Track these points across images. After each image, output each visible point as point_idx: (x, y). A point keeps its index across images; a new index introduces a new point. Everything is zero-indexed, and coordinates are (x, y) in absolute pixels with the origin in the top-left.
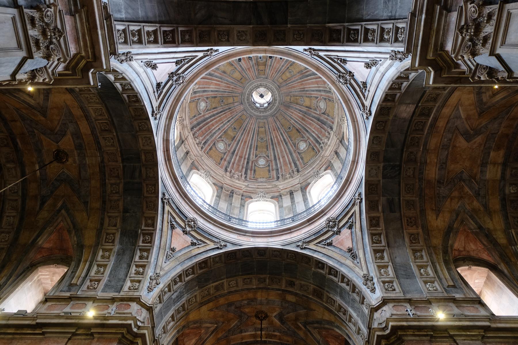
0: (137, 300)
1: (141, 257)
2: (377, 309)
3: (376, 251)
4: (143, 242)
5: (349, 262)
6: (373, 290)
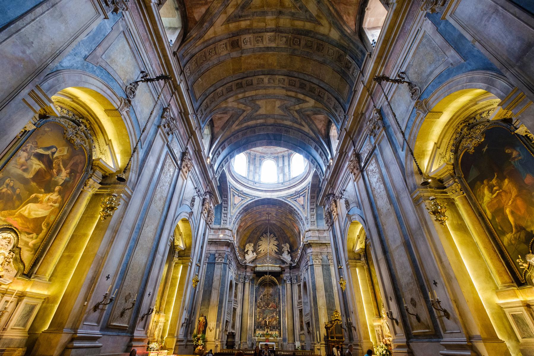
0: (227, 229)
1: (225, 210)
2: (307, 232)
3: (311, 209)
4: (224, 204)
5: (301, 209)
6: (308, 224)
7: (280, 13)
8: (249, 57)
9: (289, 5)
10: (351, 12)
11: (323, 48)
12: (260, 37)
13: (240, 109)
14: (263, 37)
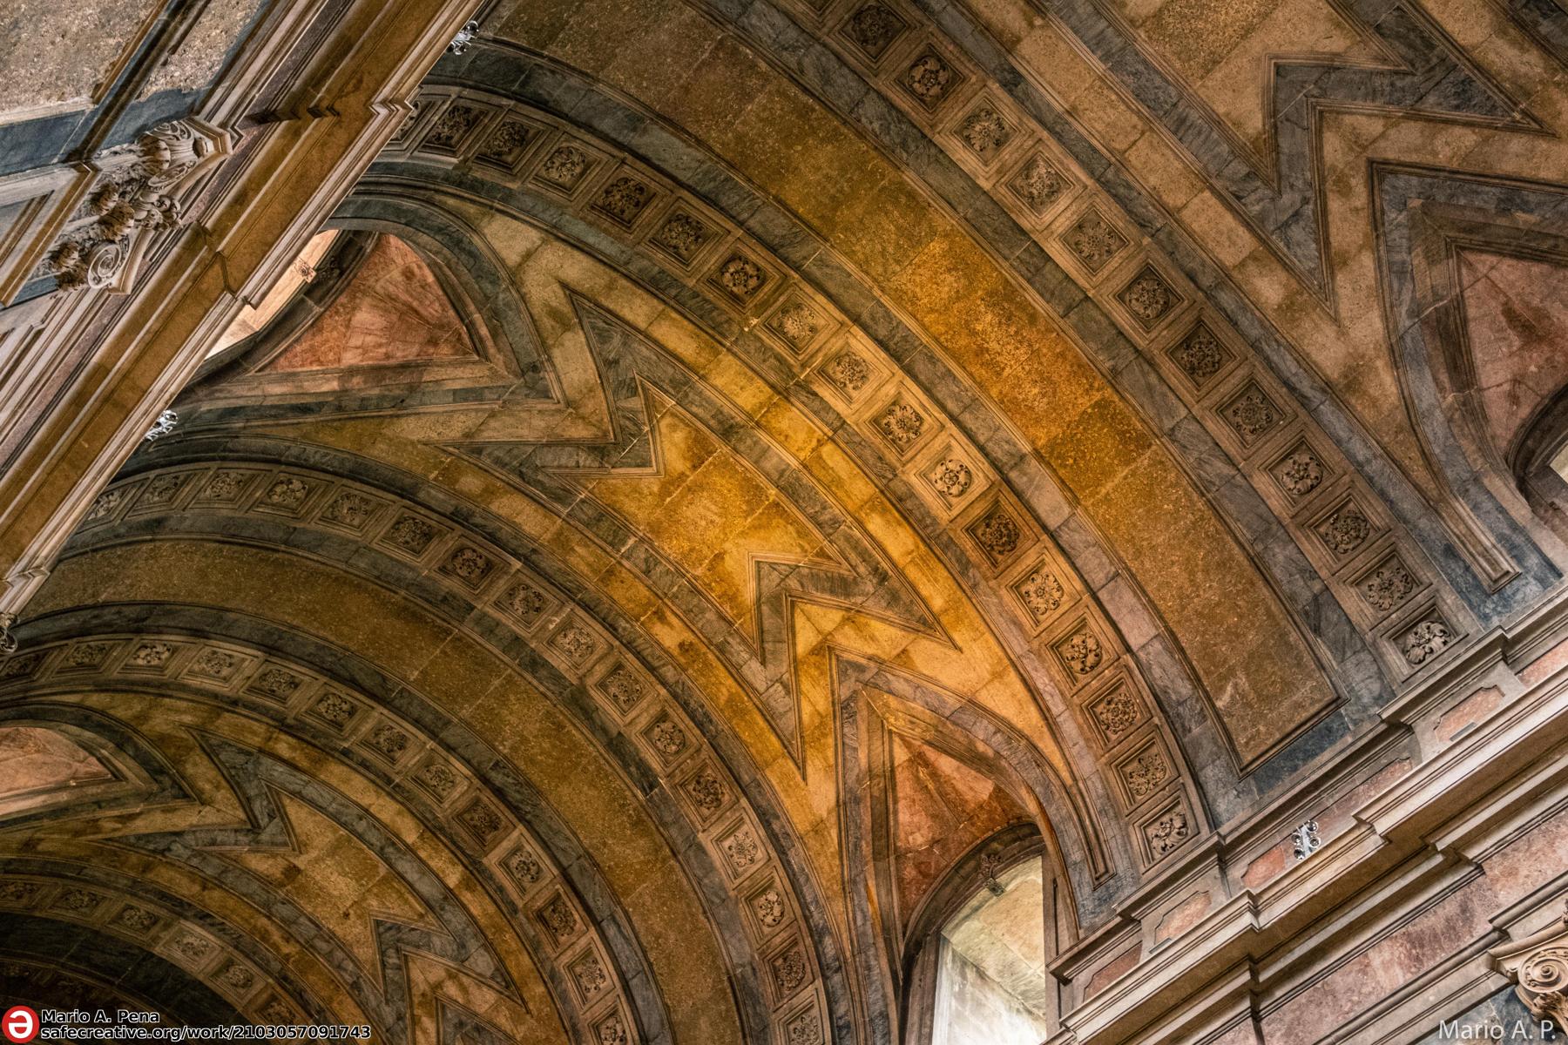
7: (728, 431)
8: (1011, 406)
9: (673, 428)
10: (396, 274)
11: (607, 192)
12: (886, 432)
13: (1376, 222)
14: (875, 421)
